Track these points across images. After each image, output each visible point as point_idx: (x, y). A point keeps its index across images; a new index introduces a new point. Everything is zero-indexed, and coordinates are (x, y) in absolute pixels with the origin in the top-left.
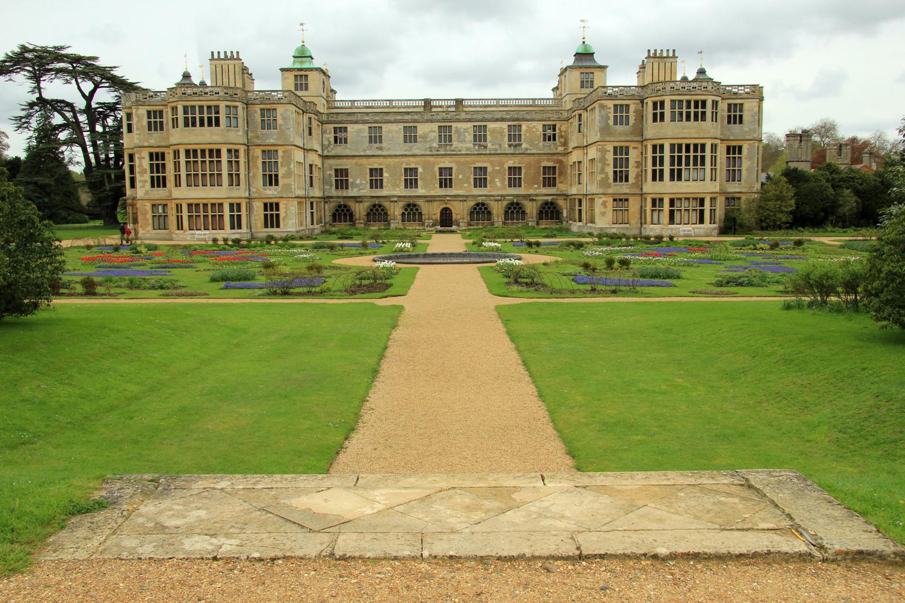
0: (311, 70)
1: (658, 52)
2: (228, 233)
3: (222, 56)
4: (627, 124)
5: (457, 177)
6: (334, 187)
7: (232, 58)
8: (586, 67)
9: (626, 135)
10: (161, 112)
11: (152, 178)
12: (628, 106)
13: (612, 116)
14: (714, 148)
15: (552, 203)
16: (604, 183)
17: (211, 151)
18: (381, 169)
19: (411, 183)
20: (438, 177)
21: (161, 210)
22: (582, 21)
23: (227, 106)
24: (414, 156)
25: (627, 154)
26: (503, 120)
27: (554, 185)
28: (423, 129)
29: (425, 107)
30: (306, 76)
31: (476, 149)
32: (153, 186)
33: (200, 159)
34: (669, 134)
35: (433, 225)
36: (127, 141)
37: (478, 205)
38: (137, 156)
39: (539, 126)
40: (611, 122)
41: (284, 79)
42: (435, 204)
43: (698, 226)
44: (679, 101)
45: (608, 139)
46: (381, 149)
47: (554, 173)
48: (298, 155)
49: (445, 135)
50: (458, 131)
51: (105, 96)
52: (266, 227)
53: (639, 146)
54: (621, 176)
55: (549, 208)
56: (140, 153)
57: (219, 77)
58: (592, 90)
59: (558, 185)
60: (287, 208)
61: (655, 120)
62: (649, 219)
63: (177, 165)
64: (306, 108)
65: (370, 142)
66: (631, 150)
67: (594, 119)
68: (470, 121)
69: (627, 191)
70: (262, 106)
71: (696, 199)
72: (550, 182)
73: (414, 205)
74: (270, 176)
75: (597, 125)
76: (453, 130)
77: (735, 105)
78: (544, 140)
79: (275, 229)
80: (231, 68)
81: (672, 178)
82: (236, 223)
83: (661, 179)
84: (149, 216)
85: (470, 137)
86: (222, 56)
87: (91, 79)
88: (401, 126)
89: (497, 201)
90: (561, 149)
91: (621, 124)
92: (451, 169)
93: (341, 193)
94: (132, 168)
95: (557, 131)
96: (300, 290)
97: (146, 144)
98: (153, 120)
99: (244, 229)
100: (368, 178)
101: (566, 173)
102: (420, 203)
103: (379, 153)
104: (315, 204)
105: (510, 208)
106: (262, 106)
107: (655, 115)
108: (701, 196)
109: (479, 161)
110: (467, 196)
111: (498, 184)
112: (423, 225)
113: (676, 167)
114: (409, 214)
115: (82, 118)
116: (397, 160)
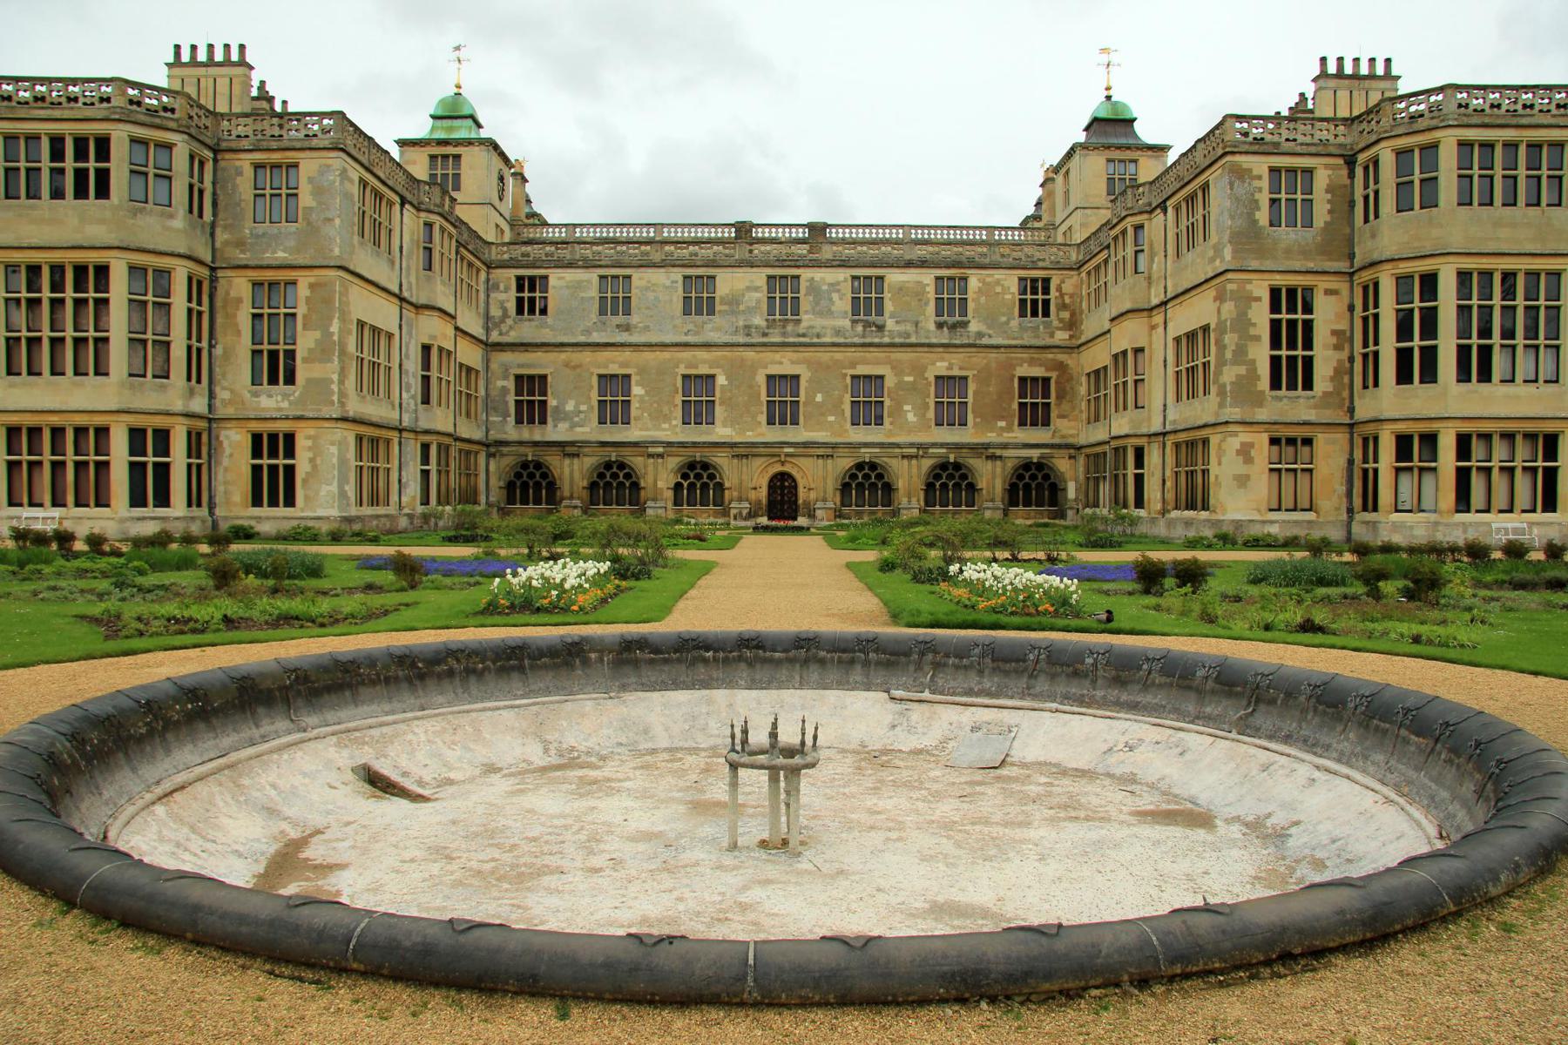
0: (469, 142)
2: (118, 519)
3: (202, 56)
4: (1308, 223)
5: (810, 400)
6: (512, 420)
7: (227, 62)
8: (1119, 148)
9: (1305, 253)
12: (1309, 172)
13: (1264, 198)
15: (1040, 466)
17: (80, 270)
18: (628, 376)
20: (764, 398)
22: (1103, 50)
23: (134, 141)
24: (707, 346)
25: (1308, 309)
26: (923, 264)
27: (1046, 423)
28: (728, 282)
30: (457, 157)
31: (857, 334)
35: (750, 515)
37: (860, 466)
39: (1010, 283)
40: (1263, 216)
43: (1539, 516)
44: (1483, 145)
45: (1254, 264)
46: (627, 328)
47: (1046, 395)
48: (385, 314)
49: (784, 297)
50: (814, 288)
52: (257, 501)
53: (1343, 287)
54: (1291, 373)
55: (1033, 477)
59: (1056, 422)
60: (316, 449)
65: (602, 312)
68: (844, 264)
69: (1311, 416)
70: (258, 156)
72: (1034, 415)
73: (706, 466)
74: (273, 355)
76: (803, 285)
78: (1022, 314)
80: (223, 85)
81: (1464, 375)
85: (842, 304)
88: (677, 275)
90: (1061, 336)
92: (796, 378)
95: (1053, 294)
100: (595, 397)
102: (721, 460)
103: (623, 337)
105: (937, 477)
106: (258, 156)
108: (1549, 427)
109: (865, 362)
110: (834, 446)
111: (911, 417)
112: (726, 513)
113: (1475, 341)
114: (692, 486)
116: (666, 355)
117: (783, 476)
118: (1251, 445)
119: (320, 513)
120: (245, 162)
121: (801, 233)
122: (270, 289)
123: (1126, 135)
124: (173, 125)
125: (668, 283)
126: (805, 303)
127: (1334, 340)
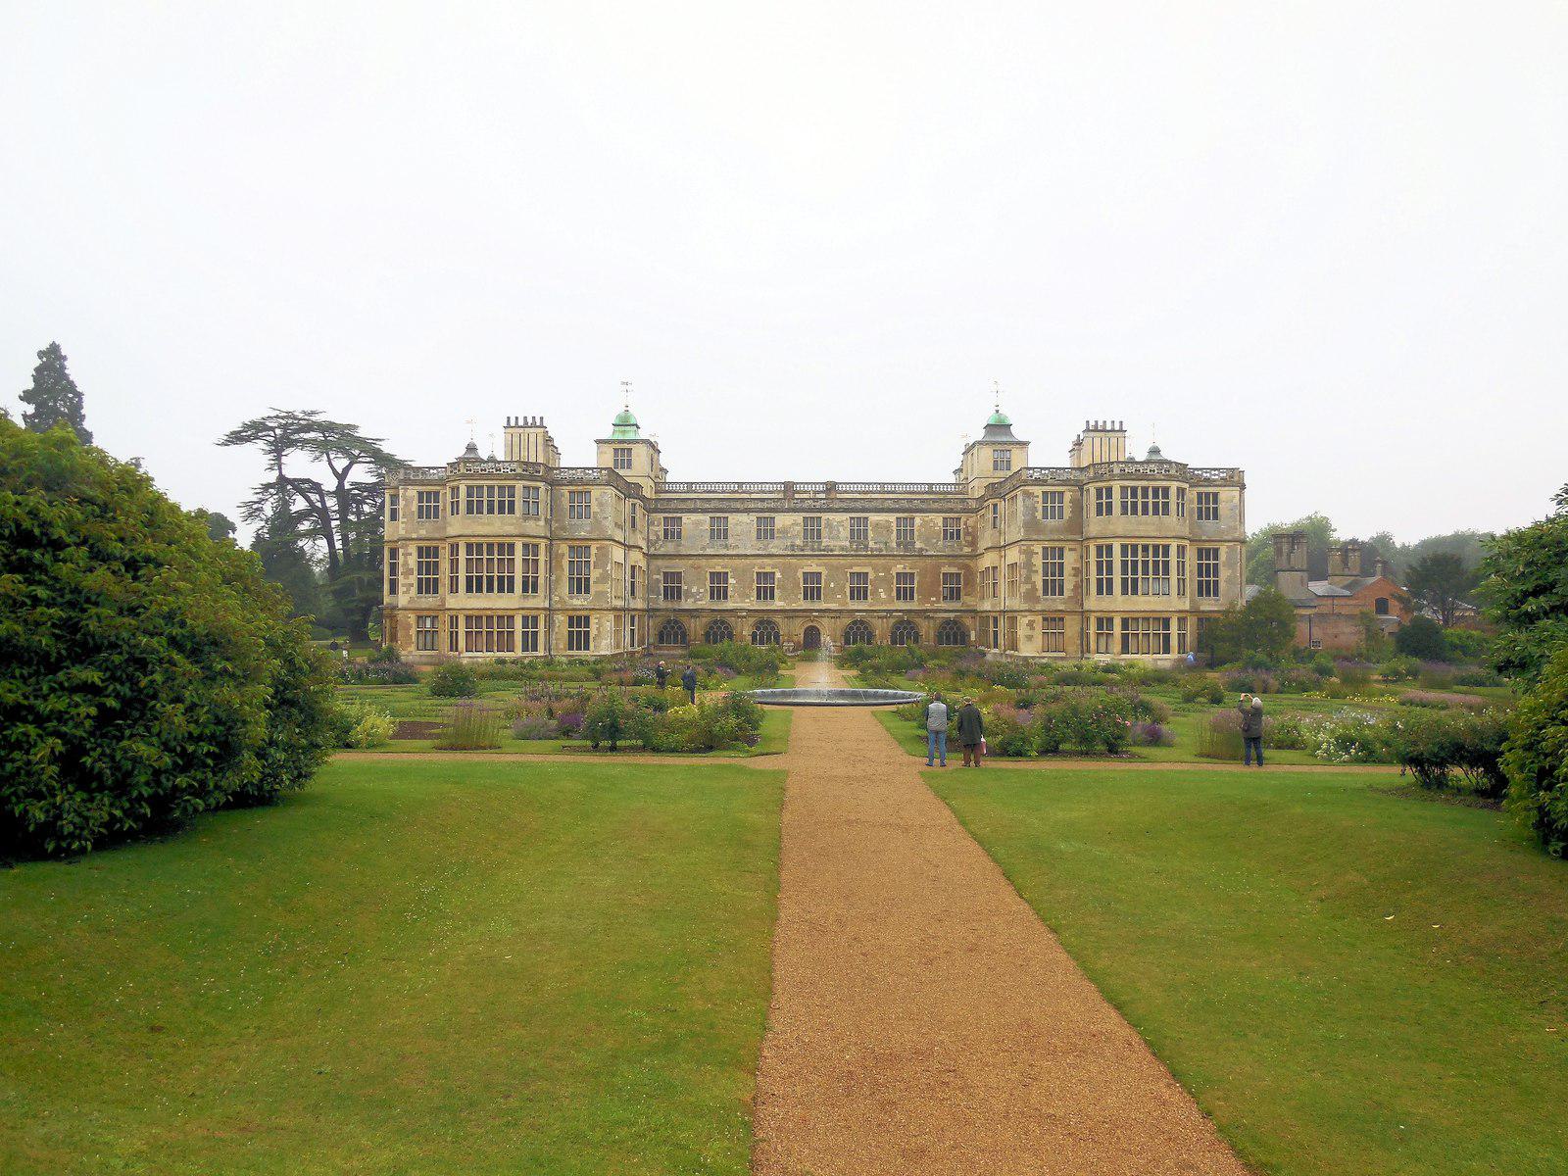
0: (636, 442)
1: (1100, 424)
3: (521, 423)
4: (1061, 517)
10: (437, 494)
11: (420, 581)
12: (1062, 494)
13: (1040, 507)
14: (1181, 550)
15: (955, 622)
16: (1031, 596)
17: (501, 546)
19: (766, 593)
20: (802, 585)
21: (428, 625)
25: (1061, 557)
29: (784, 492)
30: (630, 450)
32: (420, 591)
33: (485, 556)
34: (1120, 532)
35: (794, 650)
36: (389, 531)
37: (855, 623)
38: (401, 551)
40: (1039, 515)
41: (600, 453)
42: (799, 621)
45: (1035, 537)
48: (618, 554)
49: (812, 531)
50: (829, 525)
51: (362, 474)
52: (571, 648)
53: (1078, 547)
54: (1053, 587)
56: (405, 547)
57: (516, 449)
58: (1010, 473)
59: (964, 598)
61: (1099, 513)
62: (1093, 646)
63: (454, 564)
64: (630, 491)
66: (1067, 553)
67: (1016, 512)
69: (1061, 607)
71: (1159, 619)
72: (954, 595)
73: (769, 622)
75: (1020, 518)
77: (1207, 495)
78: (945, 538)
79: (583, 652)
81: (1125, 592)
82: (530, 642)
83: (1110, 592)
84: (413, 632)
85: (845, 533)
86: (521, 423)
87: (347, 453)
88: (753, 517)
89: (886, 617)
90: (967, 550)
91: (1053, 517)
92: (820, 573)
93: (670, 605)
94: (393, 568)
95: (962, 526)
96: (628, 743)
97: (414, 536)
98: (425, 504)
99: (541, 652)
100: (708, 584)
101: (974, 580)
102: (778, 619)
103: (724, 552)
104: (636, 618)
107: (1099, 506)
110: (840, 611)
115: (331, 503)
116: (748, 561)
117: (813, 628)
118: (1034, 621)
119: (603, 653)
120: (565, 490)
121: (822, 488)
122: (580, 549)
123: (1006, 435)
124: (539, 479)
125: (749, 521)
126: (824, 533)
127: (1073, 572)
